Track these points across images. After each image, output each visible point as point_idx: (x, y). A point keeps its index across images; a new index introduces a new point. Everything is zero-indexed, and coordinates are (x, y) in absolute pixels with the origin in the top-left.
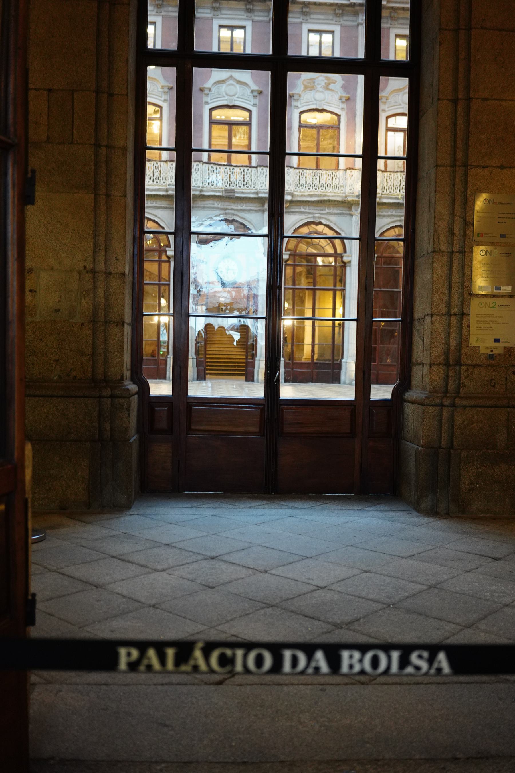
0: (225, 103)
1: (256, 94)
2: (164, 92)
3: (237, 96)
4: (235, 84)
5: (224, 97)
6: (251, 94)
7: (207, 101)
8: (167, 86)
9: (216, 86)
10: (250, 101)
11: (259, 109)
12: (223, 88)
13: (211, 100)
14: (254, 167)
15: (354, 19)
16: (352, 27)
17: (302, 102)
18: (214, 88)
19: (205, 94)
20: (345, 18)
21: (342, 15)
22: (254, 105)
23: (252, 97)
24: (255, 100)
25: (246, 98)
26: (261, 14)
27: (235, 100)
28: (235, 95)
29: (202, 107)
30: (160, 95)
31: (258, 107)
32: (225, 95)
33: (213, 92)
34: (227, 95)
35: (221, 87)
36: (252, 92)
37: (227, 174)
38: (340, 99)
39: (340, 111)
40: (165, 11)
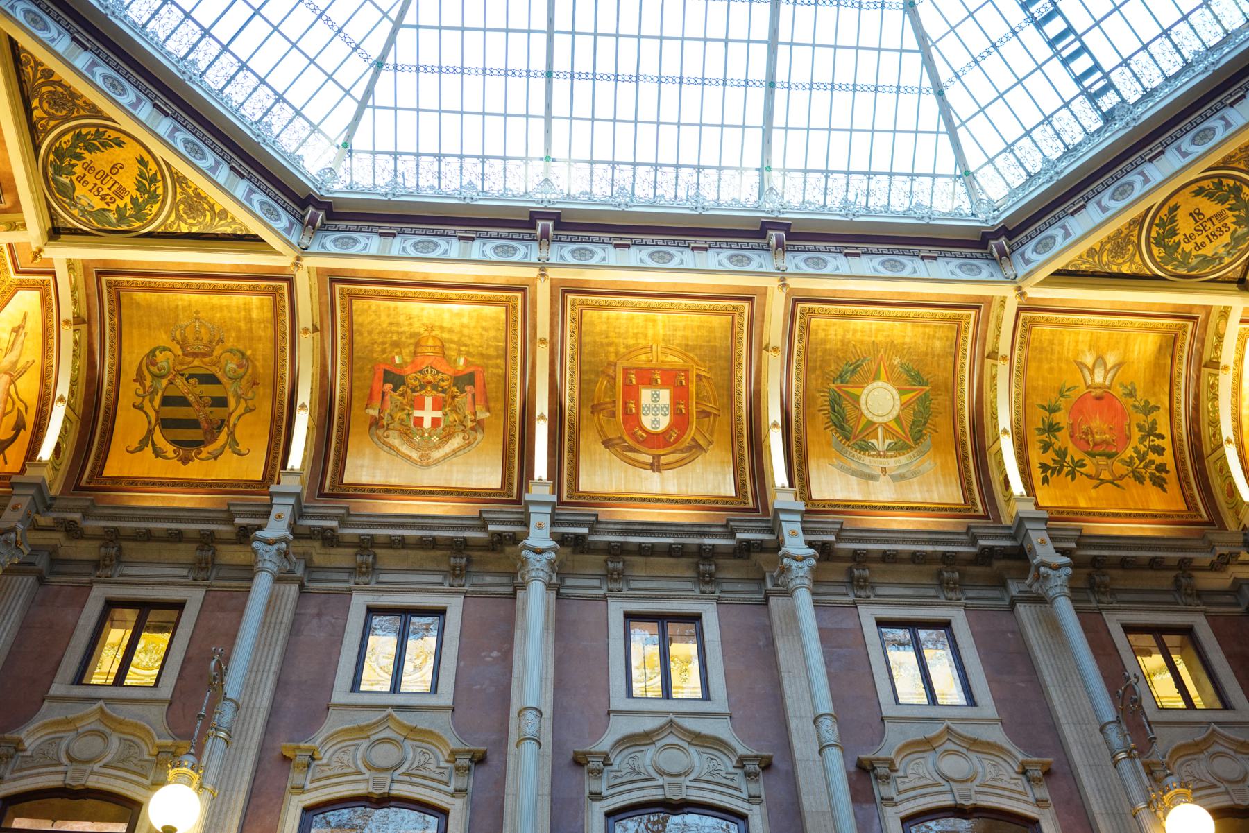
0: (657, 795)
1: (752, 767)
2: (458, 769)
3: (692, 776)
5: (653, 779)
7: (595, 788)
8: (469, 751)
9: (626, 752)
10: (739, 790)
11: (768, 810)
12: (647, 757)
13: (610, 787)
15: (996, 594)
16: (999, 609)
17: (901, 787)
19: (591, 771)
20: (970, 593)
21: (960, 586)
22: (753, 799)
26: (740, 587)
28: (686, 774)
30: (444, 778)
31: (764, 803)
32: (654, 775)
33: (615, 768)
34: (662, 773)
35: (638, 754)
36: (742, 762)
38: (1024, 773)
39: (1035, 809)
40: (473, 585)
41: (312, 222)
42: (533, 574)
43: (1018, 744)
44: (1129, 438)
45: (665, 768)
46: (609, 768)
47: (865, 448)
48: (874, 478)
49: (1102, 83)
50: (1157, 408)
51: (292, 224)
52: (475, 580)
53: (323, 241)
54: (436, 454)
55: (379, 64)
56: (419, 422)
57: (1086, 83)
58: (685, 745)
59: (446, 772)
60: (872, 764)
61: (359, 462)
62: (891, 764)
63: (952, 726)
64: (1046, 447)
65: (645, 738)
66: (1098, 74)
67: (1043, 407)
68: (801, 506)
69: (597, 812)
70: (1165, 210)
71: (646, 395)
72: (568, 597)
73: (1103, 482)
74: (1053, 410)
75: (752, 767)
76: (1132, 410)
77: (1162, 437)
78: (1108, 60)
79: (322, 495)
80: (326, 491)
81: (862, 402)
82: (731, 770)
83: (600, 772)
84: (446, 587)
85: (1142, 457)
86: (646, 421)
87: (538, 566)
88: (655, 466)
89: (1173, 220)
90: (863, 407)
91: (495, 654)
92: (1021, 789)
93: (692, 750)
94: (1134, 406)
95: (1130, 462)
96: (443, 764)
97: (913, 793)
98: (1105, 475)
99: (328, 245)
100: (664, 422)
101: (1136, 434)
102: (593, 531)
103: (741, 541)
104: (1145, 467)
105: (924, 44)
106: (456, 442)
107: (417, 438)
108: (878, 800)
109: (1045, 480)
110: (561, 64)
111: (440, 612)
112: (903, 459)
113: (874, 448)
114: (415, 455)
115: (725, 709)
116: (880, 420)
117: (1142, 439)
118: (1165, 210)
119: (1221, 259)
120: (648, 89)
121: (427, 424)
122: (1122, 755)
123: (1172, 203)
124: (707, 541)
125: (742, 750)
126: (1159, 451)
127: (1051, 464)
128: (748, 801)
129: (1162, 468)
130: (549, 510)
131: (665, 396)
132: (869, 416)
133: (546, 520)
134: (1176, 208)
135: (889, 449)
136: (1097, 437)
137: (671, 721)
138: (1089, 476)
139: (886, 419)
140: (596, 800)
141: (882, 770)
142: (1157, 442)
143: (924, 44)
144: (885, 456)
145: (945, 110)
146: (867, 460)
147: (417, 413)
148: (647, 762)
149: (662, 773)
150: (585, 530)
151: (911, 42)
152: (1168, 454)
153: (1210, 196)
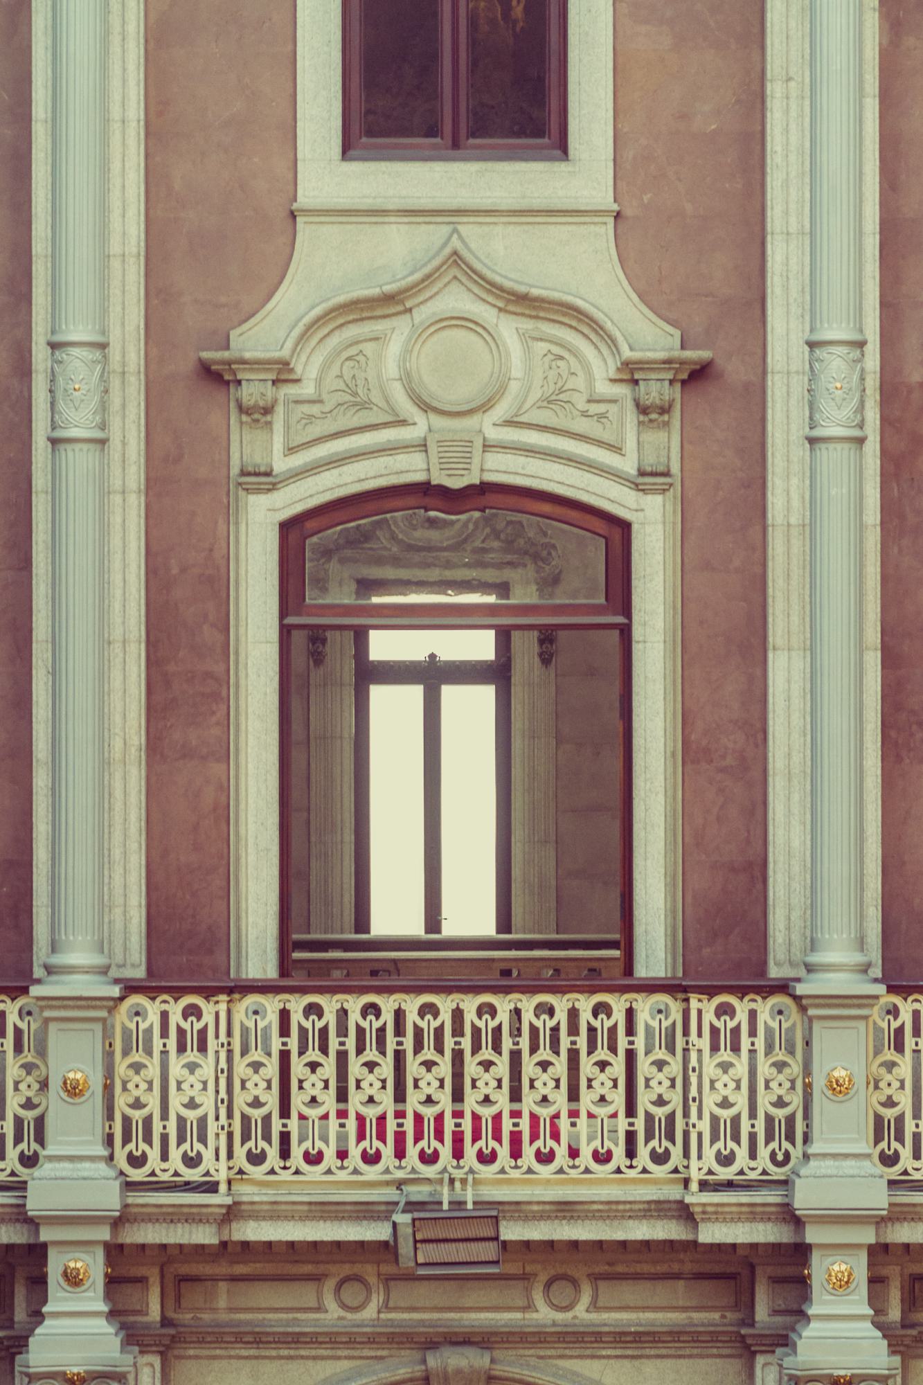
1: (656, 390)
3: (501, 410)
4: (486, 313)
5: (403, 423)
6: (623, 391)
7: (257, 459)
9: (335, 340)
10: (617, 449)
13: (291, 450)
14: (651, 987)
23: (631, 417)
24: (655, 438)
25: (581, 425)
27: (487, 447)
29: (227, 511)
32: (406, 407)
33: (307, 389)
34: (426, 407)
35: (369, 348)
36: (631, 373)
37: (440, 1049)
45: (433, 387)
82: (604, 388)
128: (637, 487)
140: (258, 491)
148: (391, 369)
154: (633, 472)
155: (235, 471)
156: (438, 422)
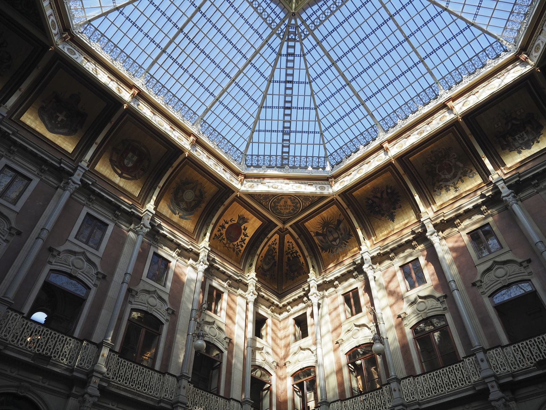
0: (69, 271)
1: (100, 276)
3: (81, 271)
5: (70, 266)
9: (66, 254)
10: (93, 281)
12: (72, 258)
13: (55, 262)
17: (136, 300)
18: (63, 255)
22: (95, 285)
28: (80, 269)
30: (4, 234)
33: (60, 257)
34: (73, 265)
39: (165, 321)
40: (45, 178)
41: (65, 38)
42: (69, 189)
43: (170, 302)
44: (238, 240)
45: (75, 264)
46: (58, 256)
47: (178, 205)
48: (175, 214)
49: (287, 157)
50: (248, 237)
51: (57, 33)
52: (47, 176)
53: (64, 46)
54: (56, 130)
55: (117, 9)
56: (58, 117)
57: (284, 154)
58: (84, 261)
59: (5, 232)
60: (132, 291)
61: (29, 116)
62: (137, 293)
63: (157, 290)
64: (219, 230)
65: (74, 253)
66: (287, 155)
67: (224, 220)
68: (154, 212)
69: (48, 267)
70: (280, 197)
71: (130, 155)
72: (73, 198)
73: (226, 246)
74: (227, 223)
75: (100, 276)
76: (242, 234)
77: (244, 243)
78: (292, 153)
79: (10, 119)
80: (12, 118)
81: (185, 193)
83: (55, 256)
84: (36, 173)
85: (238, 245)
86: (126, 161)
87: (72, 187)
88: (120, 176)
89: (280, 200)
90: (184, 194)
91: (41, 203)
92: (164, 314)
93: (86, 263)
94: (243, 233)
95: (234, 246)
96: (6, 229)
97: (138, 303)
98: (227, 245)
99: (65, 48)
100: (130, 165)
101: (240, 240)
102: (92, 184)
103: (132, 211)
104: (237, 248)
105: (258, 118)
106: (65, 131)
107: (53, 122)
108: (128, 300)
109: (214, 239)
110: (169, 51)
111: (30, 180)
112: (185, 213)
113: (180, 206)
114: (49, 126)
115: (101, 256)
116: (186, 200)
117: (240, 242)
118: (280, 197)
119: (284, 214)
120: (186, 76)
121: (59, 119)
122: (193, 319)
123: (283, 197)
124: (123, 206)
125: (99, 270)
126: (242, 246)
127: (218, 235)
129: (240, 251)
130: (84, 171)
131: (135, 158)
132: (184, 197)
133: (82, 174)
134: (283, 198)
135: (183, 209)
136: (231, 235)
137: (84, 252)
138: (224, 243)
139: (187, 201)
141: (134, 293)
142: (243, 244)
143: (258, 118)
144: (181, 210)
145: (251, 137)
146: (176, 208)
147: (58, 114)
148: (71, 260)
149: (73, 265)
150: (90, 183)
151: (255, 115)
152: (244, 248)
153: (291, 201)
154: (94, 284)
155: (48, 260)
156: (74, 268)
